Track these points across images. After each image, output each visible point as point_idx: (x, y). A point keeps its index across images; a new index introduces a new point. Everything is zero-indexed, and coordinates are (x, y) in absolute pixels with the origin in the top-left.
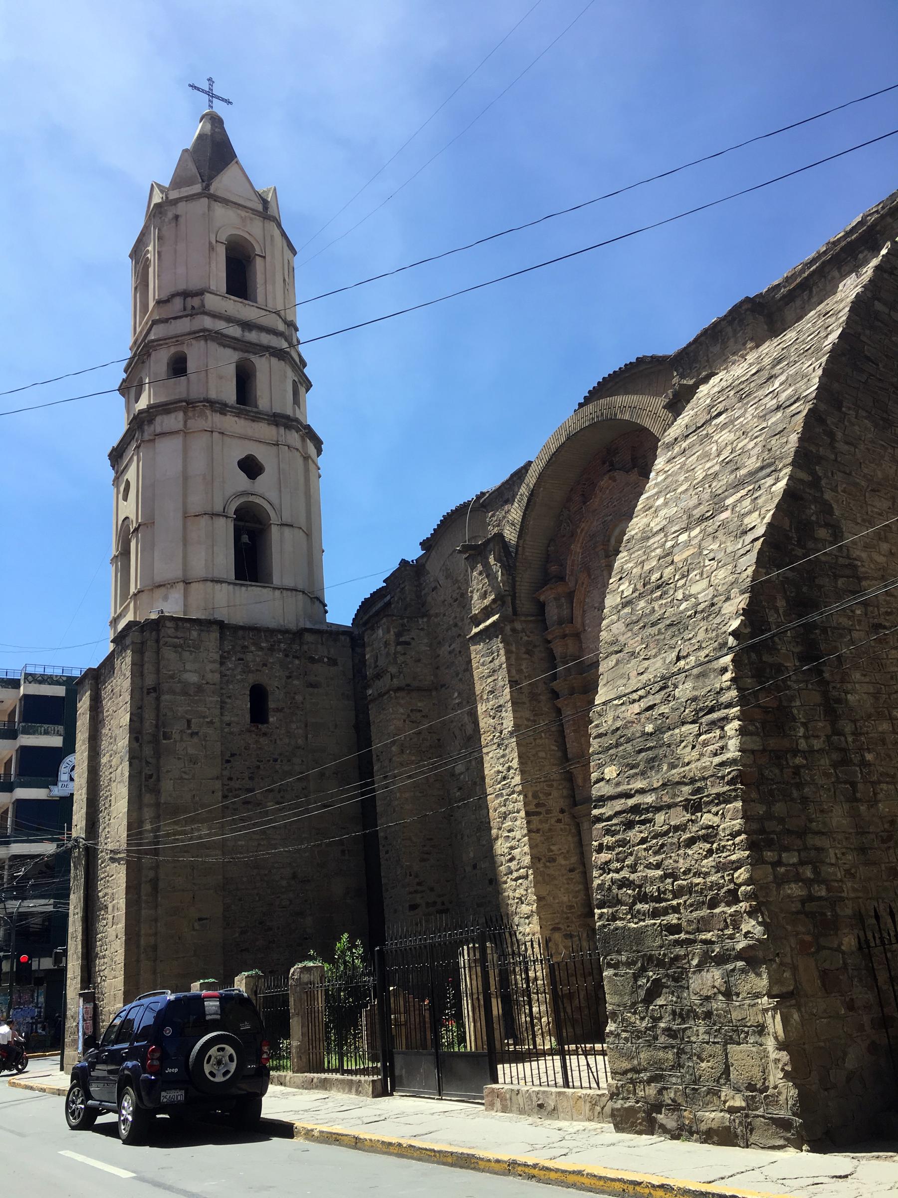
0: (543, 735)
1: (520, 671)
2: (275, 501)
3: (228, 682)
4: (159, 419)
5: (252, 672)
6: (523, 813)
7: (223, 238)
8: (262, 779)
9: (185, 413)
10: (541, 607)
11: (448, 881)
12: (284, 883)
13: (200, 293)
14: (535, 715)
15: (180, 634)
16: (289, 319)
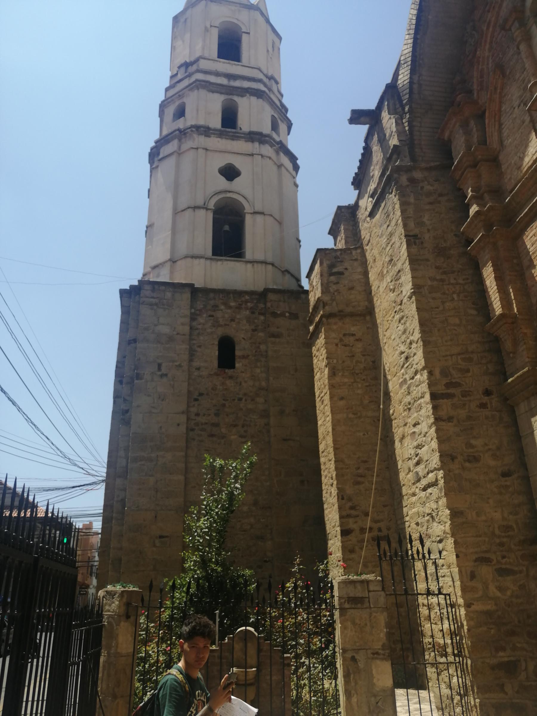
0: (455, 296)
1: (420, 224)
2: (250, 197)
3: (199, 334)
4: (162, 151)
5: (221, 326)
6: (428, 397)
7: (217, 24)
8: (227, 415)
9: (180, 140)
10: (445, 149)
11: (385, 506)
12: (245, 508)
13: (197, 61)
14: (444, 273)
15: (155, 295)
16: (270, 74)
